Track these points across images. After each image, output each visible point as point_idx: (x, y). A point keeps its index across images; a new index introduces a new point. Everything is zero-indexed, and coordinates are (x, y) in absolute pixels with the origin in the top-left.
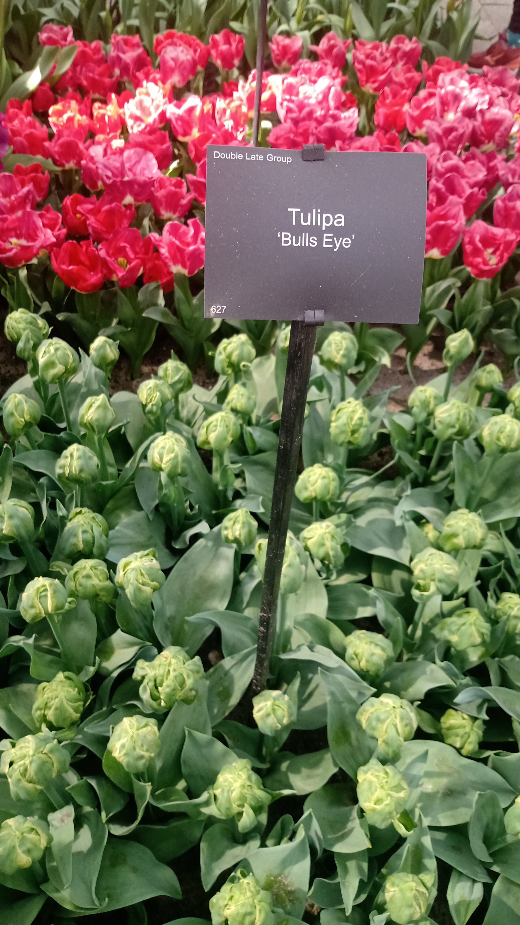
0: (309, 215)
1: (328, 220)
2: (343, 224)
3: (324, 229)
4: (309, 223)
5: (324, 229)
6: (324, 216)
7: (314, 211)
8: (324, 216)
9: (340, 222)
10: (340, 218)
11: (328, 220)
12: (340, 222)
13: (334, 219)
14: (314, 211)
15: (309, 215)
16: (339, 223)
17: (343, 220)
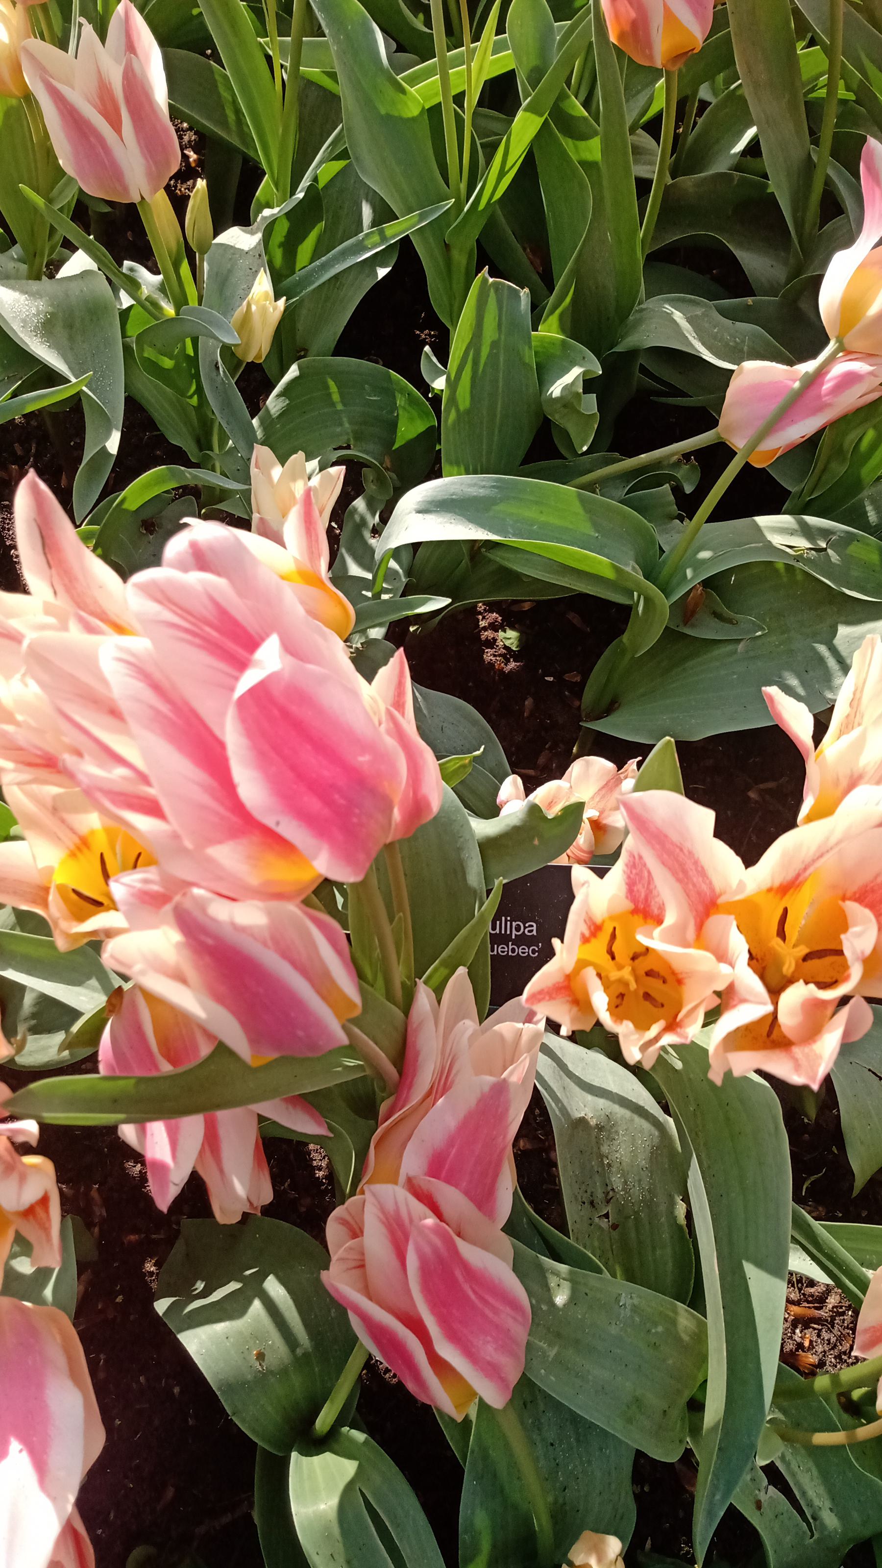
0: (498, 922)
1: (518, 928)
2: (534, 933)
3: (513, 937)
4: (498, 931)
5: (513, 937)
6: (514, 924)
7: (503, 918)
8: (514, 924)
9: (532, 931)
10: (532, 926)
11: (518, 928)
12: (532, 931)
13: (525, 928)
14: (503, 918)
15: (498, 922)
16: (529, 931)
17: (534, 928)
